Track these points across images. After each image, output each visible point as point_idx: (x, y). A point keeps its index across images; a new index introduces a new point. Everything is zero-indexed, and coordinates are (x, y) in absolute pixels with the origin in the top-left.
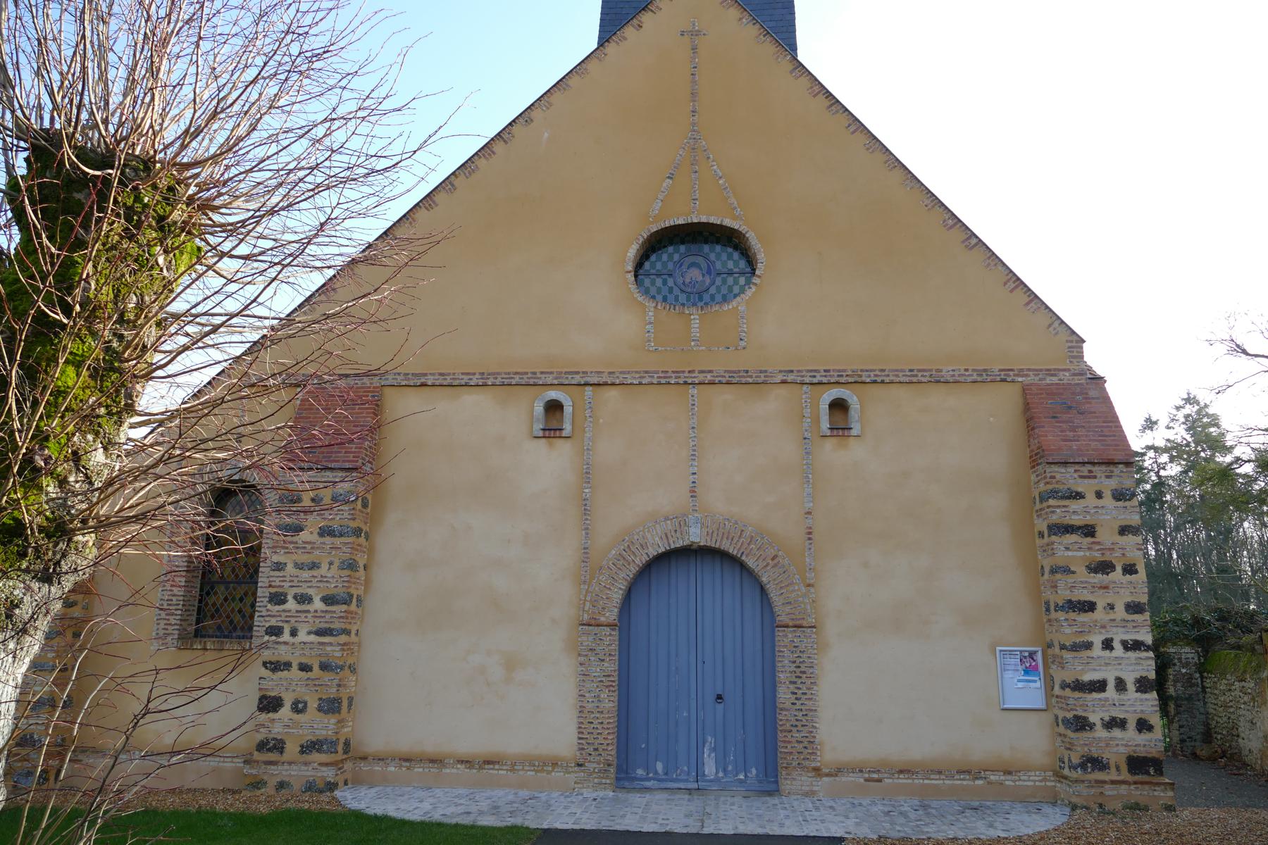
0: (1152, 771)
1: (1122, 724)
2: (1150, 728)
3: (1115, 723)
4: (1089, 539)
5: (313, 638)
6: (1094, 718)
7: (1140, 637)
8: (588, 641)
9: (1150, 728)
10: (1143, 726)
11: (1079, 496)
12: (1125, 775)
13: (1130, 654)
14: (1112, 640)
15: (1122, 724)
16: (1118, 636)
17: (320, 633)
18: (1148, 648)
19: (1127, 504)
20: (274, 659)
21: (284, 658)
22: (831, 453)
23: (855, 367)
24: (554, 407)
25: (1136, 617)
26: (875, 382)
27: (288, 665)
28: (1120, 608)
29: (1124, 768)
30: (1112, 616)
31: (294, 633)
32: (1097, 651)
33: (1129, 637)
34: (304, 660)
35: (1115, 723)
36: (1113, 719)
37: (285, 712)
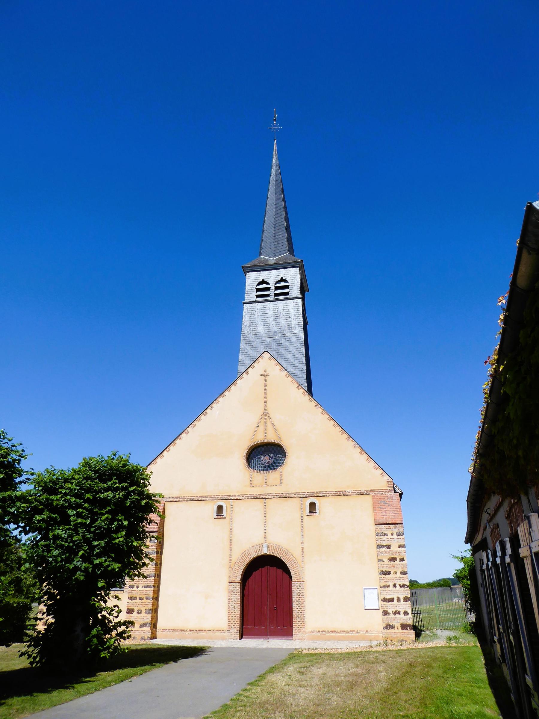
0: (408, 628)
1: (399, 613)
2: (408, 614)
3: (397, 613)
4: (389, 550)
5: (144, 589)
6: (390, 611)
7: (405, 583)
8: (231, 588)
9: (408, 614)
10: (406, 613)
11: (385, 535)
12: (400, 631)
13: (402, 589)
14: (396, 584)
15: (399, 613)
16: (398, 583)
17: (146, 587)
18: (408, 587)
19: (401, 537)
20: (131, 596)
21: (134, 596)
22: (309, 520)
23: (317, 491)
24: (220, 509)
25: (404, 576)
26: (323, 496)
27: (136, 598)
28: (399, 573)
29: (400, 628)
30: (396, 576)
31: (138, 587)
32: (391, 587)
33: (401, 583)
34: (141, 596)
35: (397, 613)
36: (396, 611)
37: (135, 614)
